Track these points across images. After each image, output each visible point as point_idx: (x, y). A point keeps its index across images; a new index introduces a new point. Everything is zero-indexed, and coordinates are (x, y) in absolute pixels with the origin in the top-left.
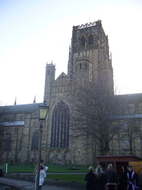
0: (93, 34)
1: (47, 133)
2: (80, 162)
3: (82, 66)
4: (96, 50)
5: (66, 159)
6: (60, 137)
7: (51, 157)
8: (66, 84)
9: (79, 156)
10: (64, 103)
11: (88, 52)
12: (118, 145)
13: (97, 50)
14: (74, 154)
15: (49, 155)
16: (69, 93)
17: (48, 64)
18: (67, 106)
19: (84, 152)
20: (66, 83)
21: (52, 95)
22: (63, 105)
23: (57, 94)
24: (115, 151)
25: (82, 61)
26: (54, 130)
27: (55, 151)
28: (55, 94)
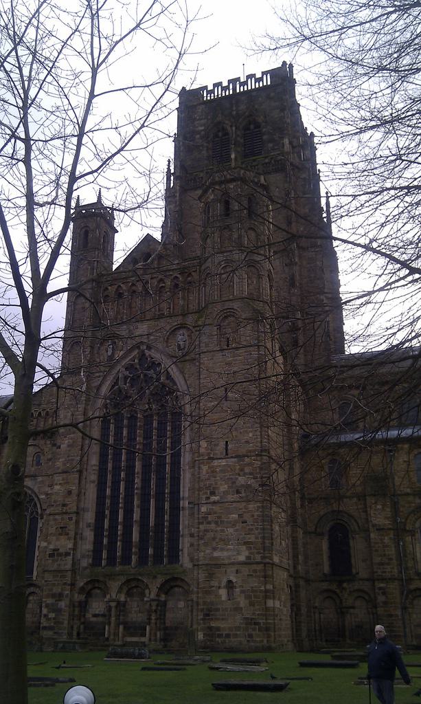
0: (260, 119)
1: (79, 501)
2: (236, 636)
5: (168, 624)
6: (136, 516)
7: (95, 616)
10: (155, 365)
12: (392, 552)
15: (83, 606)
16: (177, 321)
18: (169, 377)
19: (254, 583)
20: (161, 280)
24: (383, 580)
26: (109, 483)
27: (114, 585)
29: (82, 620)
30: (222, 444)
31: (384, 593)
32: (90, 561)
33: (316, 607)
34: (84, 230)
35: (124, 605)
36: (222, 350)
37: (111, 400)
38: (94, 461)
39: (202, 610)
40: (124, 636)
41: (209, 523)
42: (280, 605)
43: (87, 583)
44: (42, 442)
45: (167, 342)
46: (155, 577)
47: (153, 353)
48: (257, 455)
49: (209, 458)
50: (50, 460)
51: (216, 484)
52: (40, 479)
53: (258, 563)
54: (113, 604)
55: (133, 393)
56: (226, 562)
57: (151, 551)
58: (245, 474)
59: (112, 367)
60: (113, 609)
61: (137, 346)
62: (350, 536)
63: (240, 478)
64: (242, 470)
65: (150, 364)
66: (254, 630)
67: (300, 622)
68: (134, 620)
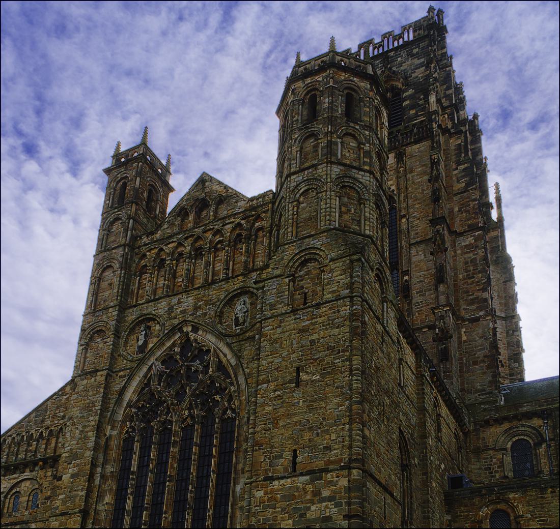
8: (218, 238)
10: (202, 352)
21: (132, 316)
22: (196, 365)
23: (163, 304)
28: (150, 309)
30: (288, 455)
36: (294, 311)
37: (139, 408)
44: (41, 473)
45: (219, 316)
47: (201, 336)
48: (342, 468)
49: (266, 479)
50: (48, 498)
51: (275, 519)
55: (168, 395)
58: (322, 500)
59: (141, 362)
63: (313, 508)
64: (316, 493)
65: (196, 352)
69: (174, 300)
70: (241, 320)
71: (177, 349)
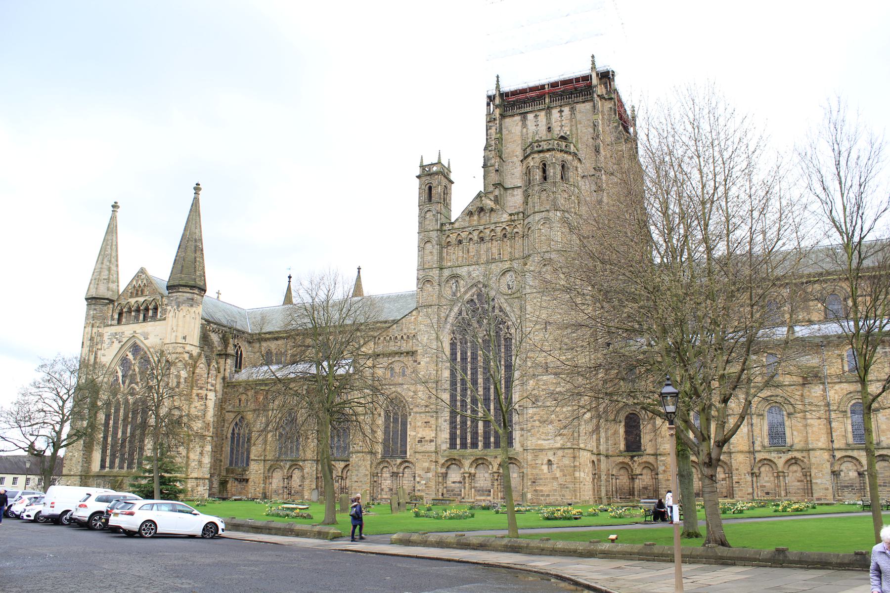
3: (551, 172)
4: (583, 105)
7: (454, 482)
8: (493, 234)
9: (549, 476)
11: (555, 113)
13: (588, 105)
14: (534, 472)
15: (445, 475)
17: (424, 164)
18: (501, 310)
25: (547, 155)
29: (445, 485)
31: (664, 465)
32: (448, 446)
33: (613, 475)
34: (428, 186)
35: (474, 476)
38: (446, 374)
39: (531, 479)
40: (475, 496)
41: (534, 421)
42: (585, 475)
43: (447, 461)
46: (496, 457)
52: (405, 387)
53: (569, 448)
54: (467, 475)
56: (547, 447)
57: (492, 439)
60: (467, 478)
61: (475, 285)
62: (641, 423)
66: (566, 491)
67: (600, 486)
68: (482, 485)
69: (471, 268)
70: (511, 287)
71: (475, 297)
